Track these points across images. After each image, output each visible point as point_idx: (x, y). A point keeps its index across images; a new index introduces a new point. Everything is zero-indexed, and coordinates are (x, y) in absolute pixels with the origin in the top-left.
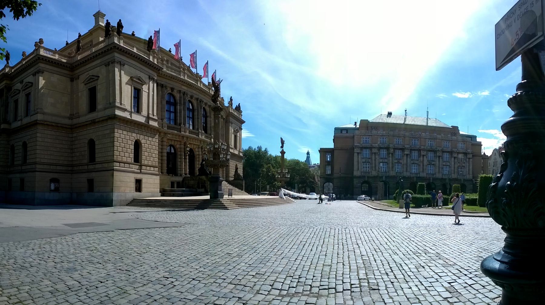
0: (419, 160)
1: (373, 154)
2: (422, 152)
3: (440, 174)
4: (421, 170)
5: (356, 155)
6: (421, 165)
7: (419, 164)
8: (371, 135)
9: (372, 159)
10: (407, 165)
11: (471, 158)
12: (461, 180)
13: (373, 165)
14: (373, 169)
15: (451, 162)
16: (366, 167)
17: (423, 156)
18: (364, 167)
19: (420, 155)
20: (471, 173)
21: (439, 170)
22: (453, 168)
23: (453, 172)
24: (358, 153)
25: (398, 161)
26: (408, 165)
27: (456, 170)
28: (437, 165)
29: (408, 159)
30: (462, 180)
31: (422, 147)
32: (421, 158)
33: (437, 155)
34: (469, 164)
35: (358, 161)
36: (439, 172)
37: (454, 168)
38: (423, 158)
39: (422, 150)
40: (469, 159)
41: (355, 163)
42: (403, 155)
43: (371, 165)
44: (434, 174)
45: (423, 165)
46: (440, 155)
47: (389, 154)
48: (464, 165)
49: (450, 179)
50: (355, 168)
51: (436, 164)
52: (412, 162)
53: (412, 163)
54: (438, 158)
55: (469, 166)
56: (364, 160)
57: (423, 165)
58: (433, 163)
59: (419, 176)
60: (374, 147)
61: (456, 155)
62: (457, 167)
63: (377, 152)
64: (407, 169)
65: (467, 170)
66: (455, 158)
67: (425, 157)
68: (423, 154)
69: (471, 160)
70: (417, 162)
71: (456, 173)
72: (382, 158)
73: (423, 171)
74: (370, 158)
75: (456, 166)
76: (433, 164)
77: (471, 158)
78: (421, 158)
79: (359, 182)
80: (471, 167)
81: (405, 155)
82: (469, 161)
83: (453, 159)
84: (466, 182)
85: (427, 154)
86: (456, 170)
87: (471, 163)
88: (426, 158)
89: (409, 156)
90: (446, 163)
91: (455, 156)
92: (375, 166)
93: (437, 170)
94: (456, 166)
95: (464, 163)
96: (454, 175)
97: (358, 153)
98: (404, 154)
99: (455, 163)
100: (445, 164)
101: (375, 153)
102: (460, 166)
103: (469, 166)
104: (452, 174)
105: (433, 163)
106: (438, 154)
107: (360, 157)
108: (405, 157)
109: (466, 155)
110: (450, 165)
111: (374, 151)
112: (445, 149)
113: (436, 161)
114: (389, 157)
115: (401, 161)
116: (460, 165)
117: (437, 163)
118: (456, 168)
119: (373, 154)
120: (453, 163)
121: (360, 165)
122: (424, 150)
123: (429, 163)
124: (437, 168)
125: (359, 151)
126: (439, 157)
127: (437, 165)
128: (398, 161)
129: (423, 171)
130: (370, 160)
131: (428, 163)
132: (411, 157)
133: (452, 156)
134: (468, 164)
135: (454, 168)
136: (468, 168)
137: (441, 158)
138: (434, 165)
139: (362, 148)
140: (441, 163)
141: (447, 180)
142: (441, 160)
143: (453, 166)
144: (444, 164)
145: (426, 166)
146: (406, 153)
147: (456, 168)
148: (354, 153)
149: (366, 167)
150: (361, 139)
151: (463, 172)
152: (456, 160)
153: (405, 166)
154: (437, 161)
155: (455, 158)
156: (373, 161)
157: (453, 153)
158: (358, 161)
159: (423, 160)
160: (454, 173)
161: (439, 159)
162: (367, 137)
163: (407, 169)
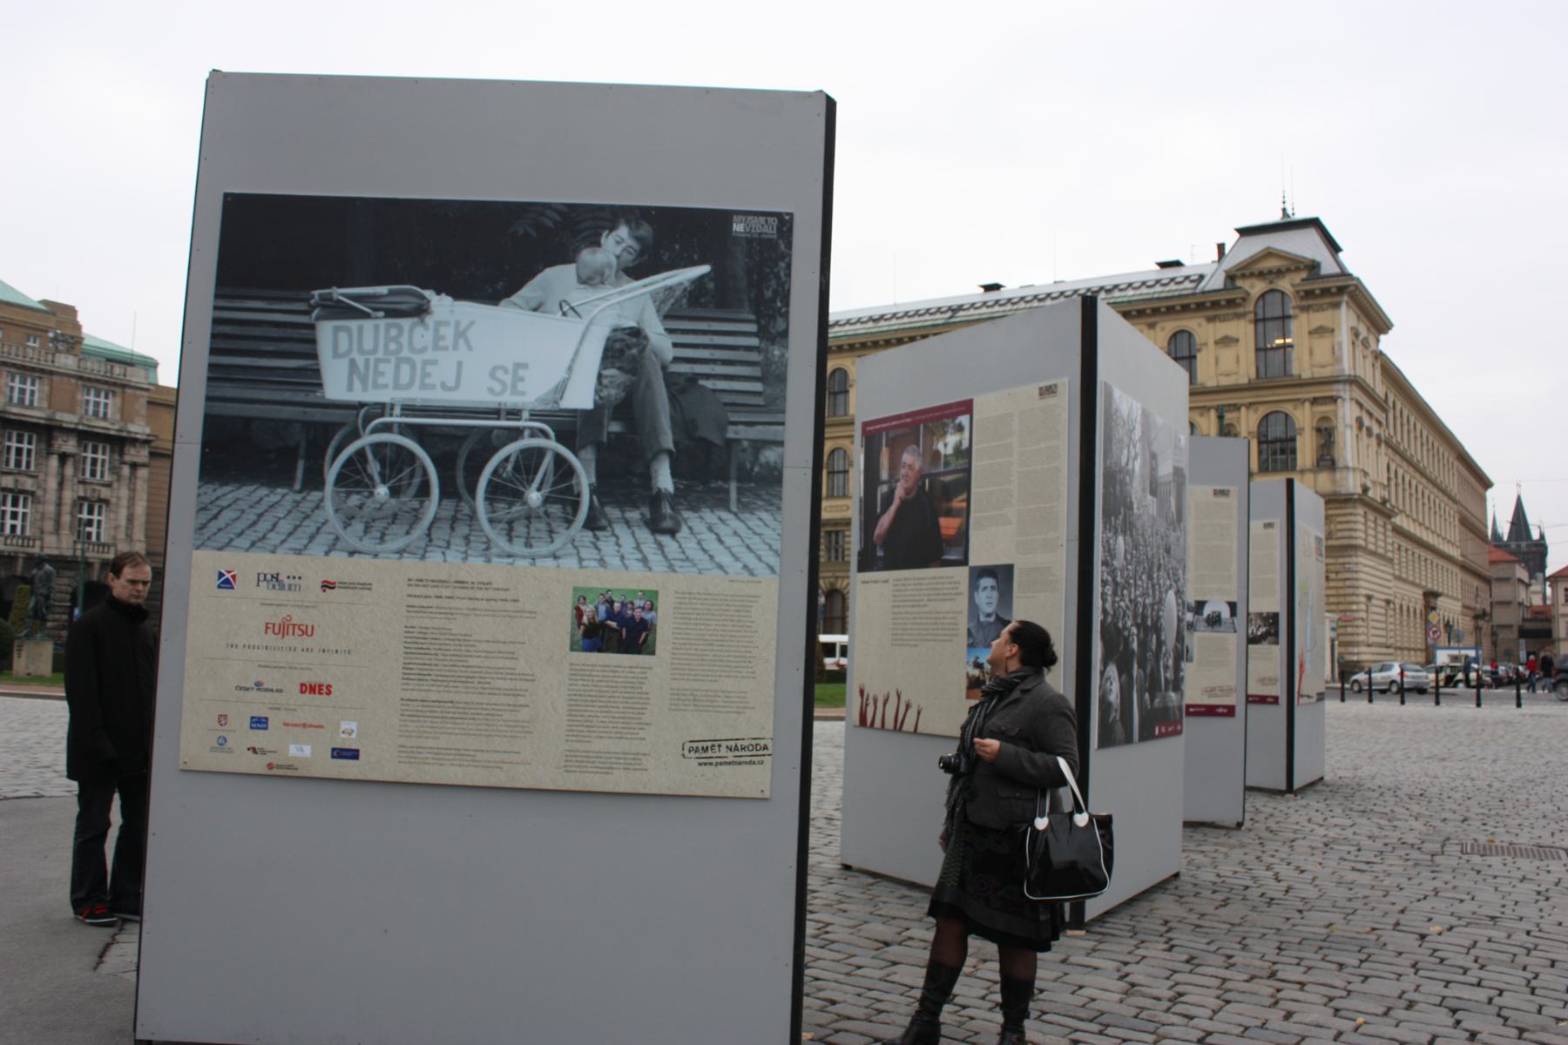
11: (144, 465)
12: (89, 565)
15: (42, 476)
20: (139, 534)
22: (51, 508)
23: (49, 525)
27: (66, 518)
30: (97, 566)
34: (133, 490)
37: (59, 504)
40: (134, 466)
48: (105, 493)
55: (132, 501)
61: (70, 446)
62: (74, 504)
65: (123, 522)
66: (63, 458)
69: (143, 473)
71: (65, 532)
75: (68, 496)
77: (144, 465)
80: (140, 509)
82: (133, 475)
83: (54, 462)
86: (66, 518)
87: (141, 486)
90: (17, 481)
94: (68, 496)
95: (109, 485)
99: (61, 484)
103: (132, 501)
109: (117, 449)
110: (39, 493)
112: (15, 410)
116: (85, 491)
118: (66, 509)
120: (52, 484)
133: (50, 445)
134: (124, 492)
135: (59, 504)
136: (123, 512)
141: (20, 562)
143: (52, 496)
147: (66, 509)
152: (69, 470)
155: (63, 458)
157: (56, 434)
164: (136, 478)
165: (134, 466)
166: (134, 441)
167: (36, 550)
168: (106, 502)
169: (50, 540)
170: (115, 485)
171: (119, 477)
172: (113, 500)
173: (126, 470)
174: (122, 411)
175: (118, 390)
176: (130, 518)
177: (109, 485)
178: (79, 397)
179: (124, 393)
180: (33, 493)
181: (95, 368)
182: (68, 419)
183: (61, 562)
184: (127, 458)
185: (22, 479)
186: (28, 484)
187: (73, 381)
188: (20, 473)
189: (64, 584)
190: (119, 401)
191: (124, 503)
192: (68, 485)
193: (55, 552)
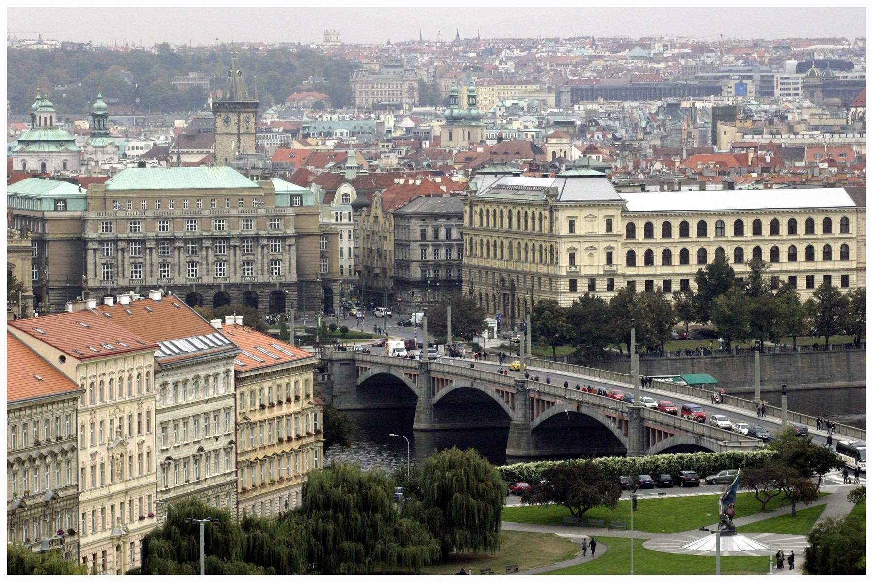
1: (120, 251)
2: (204, 241)
3: (237, 277)
4: (205, 272)
5: (90, 253)
6: (204, 263)
7: (200, 261)
8: (116, 219)
9: (117, 259)
10: (179, 265)
11: (294, 245)
13: (120, 269)
14: (120, 275)
16: (108, 273)
17: (207, 248)
18: (104, 272)
20: (294, 271)
21: (235, 270)
22: (260, 266)
23: (260, 272)
24: (95, 250)
25: (164, 260)
26: (182, 265)
27: (266, 269)
28: (232, 262)
29: (182, 256)
30: (278, 285)
31: (205, 234)
32: (204, 253)
35: (95, 264)
36: (235, 274)
37: (263, 264)
39: (204, 238)
40: (290, 246)
41: (90, 267)
42: (172, 248)
44: (227, 278)
45: (207, 264)
46: (237, 244)
47: (146, 249)
48: (280, 257)
49: (254, 285)
50: (90, 274)
52: (188, 259)
53: (188, 260)
54: (232, 251)
56: (104, 261)
57: (207, 264)
59: (200, 282)
60: (121, 240)
63: (126, 247)
64: (180, 273)
66: (263, 247)
67: (210, 250)
68: (207, 245)
69: (294, 248)
70: (196, 259)
71: (266, 273)
72: (133, 257)
73: (208, 274)
74: (114, 258)
75: (266, 260)
76: (224, 259)
77: (294, 245)
78: (204, 253)
81: (176, 249)
83: (260, 249)
84: (285, 288)
86: (266, 269)
88: (213, 250)
89: (182, 251)
92: (123, 270)
93: (232, 269)
94: (266, 260)
95: (282, 254)
96: (261, 276)
97: (95, 250)
98: (175, 248)
99: (263, 256)
101: (123, 249)
102: (273, 260)
104: (259, 276)
105: (224, 258)
106: (233, 243)
107: (97, 256)
108: (176, 253)
111: (121, 245)
114: (146, 254)
115: (169, 260)
117: (232, 257)
118: (265, 265)
119: (120, 251)
120: (260, 257)
121: (98, 269)
122: (207, 238)
126: (235, 247)
127: (232, 262)
128: (164, 260)
129: (208, 274)
133: (258, 243)
134: (287, 256)
136: (287, 263)
137: (237, 249)
138: (226, 261)
139: (101, 242)
140: (238, 258)
142: (238, 252)
143: (260, 262)
144: (245, 258)
145: (213, 264)
146: (177, 245)
147: (265, 265)
148: (86, 250)
149: (108, 273)
152: (265, 251)
153: (176, 268)
154: (232, 254)
155: (263, 247)
156: (120, 263)
158: (95, 264)
159: (207, 255)
160: (263, 274)
161: (235, 250)
162: (109, 221)
163: (180, 273)
166: (289, 237)
167: (256, 281)
168: (281, 260)
169: (260, 277)
173: (287, 248)
174: (284, 225)
176: (290, 265)
177: (282, 254)
182: (262, 233)
183: (264, 285)
184: (287, 243)
185: (249, 256)
186: (252, 258)
188: (248, 254)
189: (267, 291)
190: (283, 222)
191: (287, 260)
192: (265, 256)
193: (262, 281)
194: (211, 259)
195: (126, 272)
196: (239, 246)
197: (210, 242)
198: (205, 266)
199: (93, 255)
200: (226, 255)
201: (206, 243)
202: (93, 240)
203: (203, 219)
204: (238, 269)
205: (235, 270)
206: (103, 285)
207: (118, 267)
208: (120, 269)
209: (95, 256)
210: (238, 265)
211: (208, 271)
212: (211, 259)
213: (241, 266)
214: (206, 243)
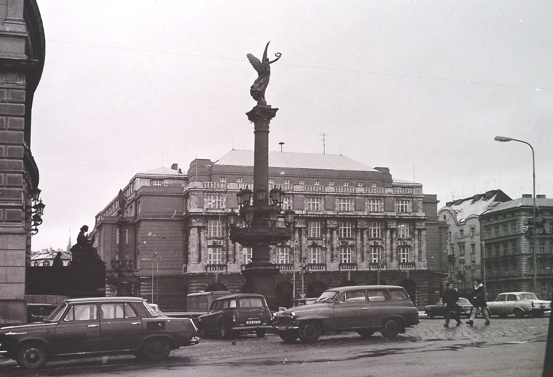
0: (324, 239)
4: (329, 257)
5: (193, 232)
6: (329, 247)
13: (230, 253)
15: (384, 239)
17: (332, 230)
19: (324, 230)
22: (389, 252)
26: (303, 248)
27: (395, 255)
28: (359, 247)
29: (304, 238)
30: (408, 274)
32: (328, 235)
33: (358, 227)
34: (420, 240)
37: (392, 249)
38: (332, 234)
40: (420, 230)
43: (225, 253)
45: (332, 249)
48: (409, 243)
51: (356, 244)
55: (420, 246)
58: (350, 242)
61: (394, 226)
62: (397, 249)
65: (417, 254)
66: (392, 231)
67: (335, 232)
68: (331, 226)
69: (424, 233)
74: (222, 239)
75: (395, 246)
78: (328, 235)
79: (200, 286)
85: (338, 227)
87: (423, 238)
90: (375, 242)
91: (392, 227)
92: (235, 254)
93: (359, 255)
94: (395, 246)
97: (199, 229)
99: (392, 242)
100: (373, 244)
103: (420, 246)
105: (350, 242)
109: (412, 224)
110: (384, 246)
113: (356, 240)
117: (359, 242)
118: (394, 251)
120: (388, 242)
121: (202, 252)
123: (342, 242)
124: (359, 251)
125: (201, 224)
127: (359, 247)
130: (222, 241)
131: (341, 245)
132: (307, 233)
134: (416, 242)
135: (392, 249)
136: (417, 250)
137: (365, 232)
138: (352, 246)
140: (365, 241)
142: (365, 236)
143: (388, 247)
144: (372, 243)
145: (338, 249)
147: (394, 251)
150: (205, 199)
151: (407, 257)
155: (392, 231)
159: (332, 238)
161: (362, 235)
164: (421, 235)
165: (420, 230)
168: (410, 246)
170: (413, 239)
171: (414, 236)
172: (412, 246)
173: (416, 233)
174: (413, 208)
175: (411, 200)
176: (420, 252)
178: (395, 205)
179: (413, 200)
180: (381, 247)
181: (399, 191)
187: (393, 199)
188: (376, 239)
191: (417, 246)
192: (394, 242)
194: (336, 242)
195: (238, 256)
196: (366, 229)
197: (335, 223)
198: (329, 250)
199: (197, 235)
200: (352, 239)
201: (332, 224)
202: (197, 216)
203: (326, 197)
204: (365, 255)
205: (362, 256)
206: (209, 271)
207: (228, 249)
208: (230, 253)
209: (200, 236)
210: (365, 249)
211: (332, 257)
212: (336, 242)
213: (368, 252)
214: (332, 224)
